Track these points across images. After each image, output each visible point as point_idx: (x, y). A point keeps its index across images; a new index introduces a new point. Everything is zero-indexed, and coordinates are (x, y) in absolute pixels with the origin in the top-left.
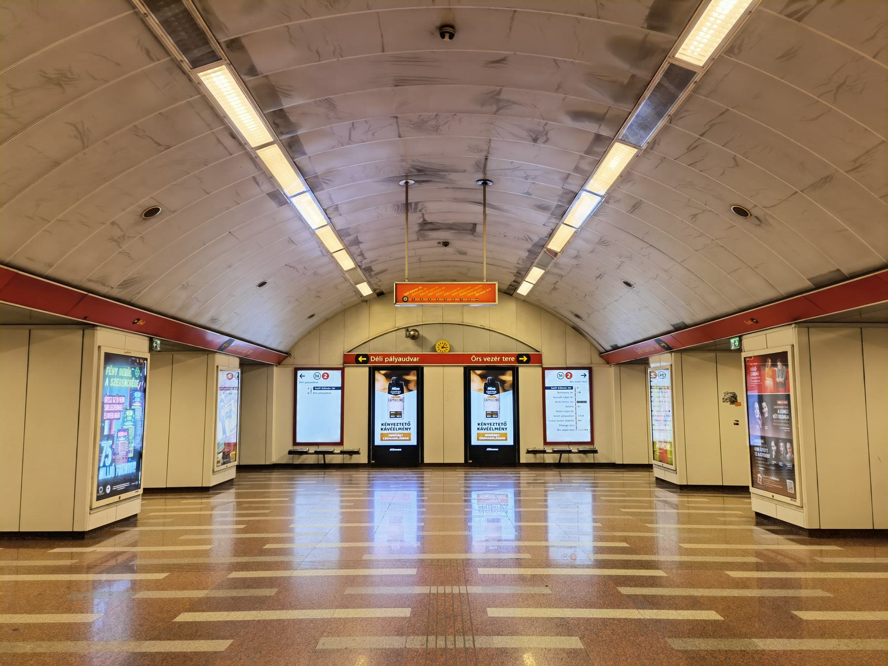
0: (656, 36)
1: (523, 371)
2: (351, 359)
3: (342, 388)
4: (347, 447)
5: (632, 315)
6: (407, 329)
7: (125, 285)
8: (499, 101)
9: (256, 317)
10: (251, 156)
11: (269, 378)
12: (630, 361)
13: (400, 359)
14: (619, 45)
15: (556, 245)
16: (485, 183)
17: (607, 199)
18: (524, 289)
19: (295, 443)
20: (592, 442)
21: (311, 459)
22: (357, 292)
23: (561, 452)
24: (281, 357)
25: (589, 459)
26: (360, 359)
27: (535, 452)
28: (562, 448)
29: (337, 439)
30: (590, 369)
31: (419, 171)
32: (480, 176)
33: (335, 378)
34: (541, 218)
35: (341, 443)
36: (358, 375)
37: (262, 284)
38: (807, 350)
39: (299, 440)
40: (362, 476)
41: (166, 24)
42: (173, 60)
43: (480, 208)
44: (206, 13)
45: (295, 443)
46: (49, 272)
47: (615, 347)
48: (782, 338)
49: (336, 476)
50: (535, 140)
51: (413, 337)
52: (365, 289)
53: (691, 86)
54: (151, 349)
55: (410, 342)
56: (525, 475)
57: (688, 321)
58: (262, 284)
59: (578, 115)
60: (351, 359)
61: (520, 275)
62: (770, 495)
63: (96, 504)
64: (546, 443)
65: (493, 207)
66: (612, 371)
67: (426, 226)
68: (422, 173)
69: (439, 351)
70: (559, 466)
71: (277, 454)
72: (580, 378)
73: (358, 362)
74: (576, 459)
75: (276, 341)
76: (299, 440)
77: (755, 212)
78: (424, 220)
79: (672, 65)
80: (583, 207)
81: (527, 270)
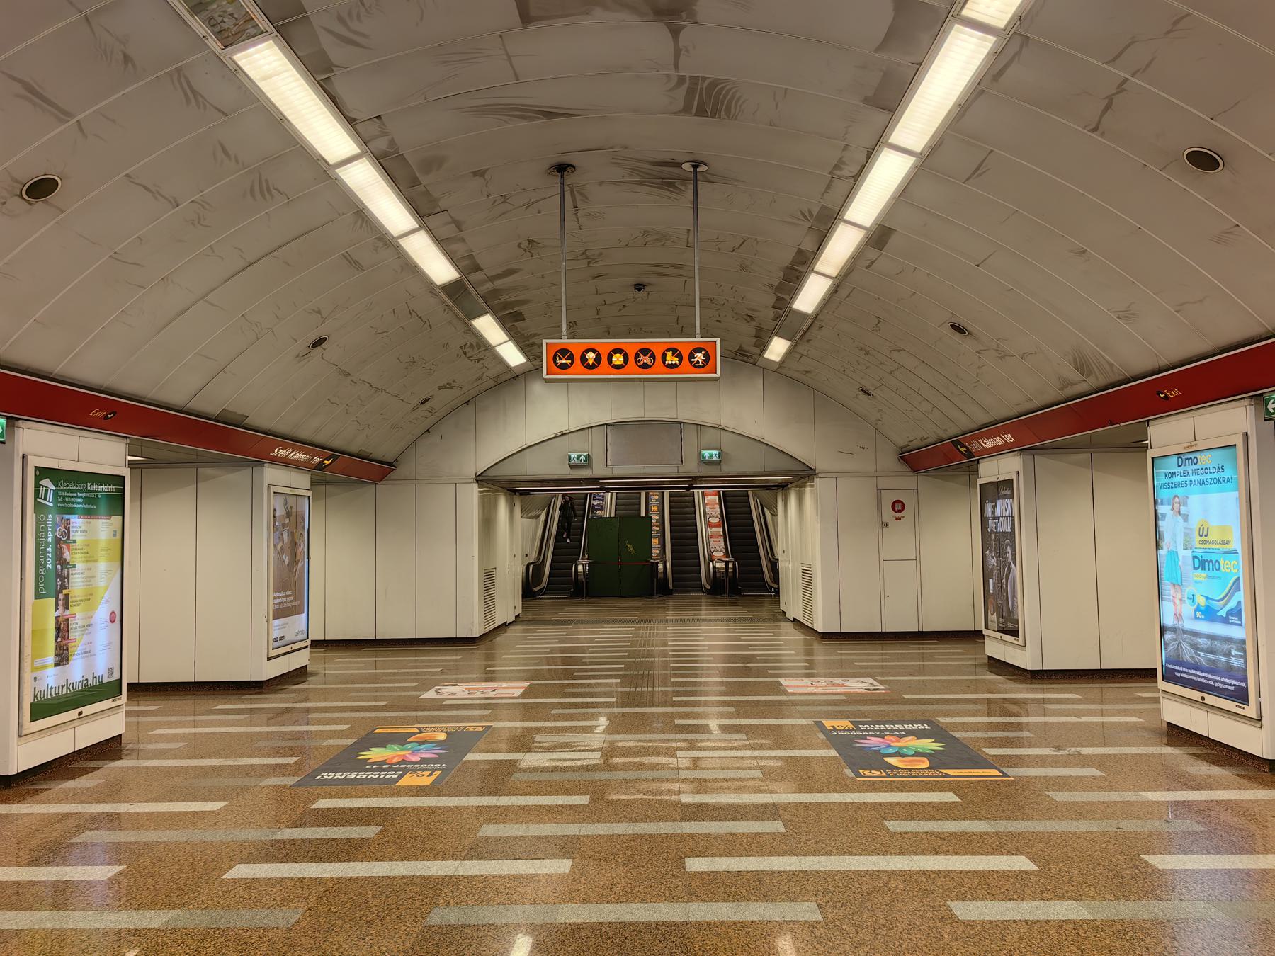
31: (672, 185)
32: (570, 179)
78: (675, 33)
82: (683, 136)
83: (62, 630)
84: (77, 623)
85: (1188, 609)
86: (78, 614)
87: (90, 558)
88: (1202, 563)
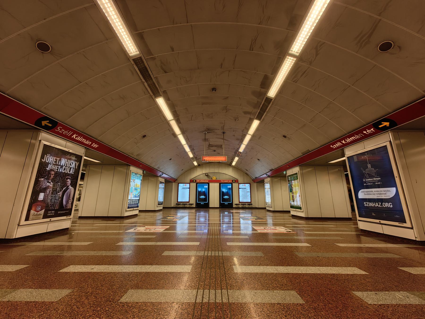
0: (263, 90)
1: (234, 184)
2: (192, 181)
3: (189, 188)
4: (190, 203)
5: (260, 170)
6: (205, 174)
7: (138, 155)
8: (227, 109)
9: (169, 171)
10: (167, 123)
11: (172, 186)
12: (260, 182)
14: (254, 93)
15: (241, 150)
16: (224, 133)
17: (253, 136)
18: (234, 164)
19: (178, 202)
20: (251, 202)
21: (181, 206)
22: (193, 164)
23: (243, 204)
24: (175, 180)
25: (250, 206)
27: (237, 204)
28: (243, 203)
29: (188, 201)
30: (250, 184)
33: (188, 186)
34: (237, 142)
35: (189, 202)
36: (194, 185)
37: (170, 159)
38: (302, 175)
39: (179, 201)
40: (194, 211)
41: (149, 85)
42: (150, 95)
43: (223, 140)
44: (158, 82)
45: (178, 202)
46: (119, 149)
47: (256, 178)
48: (296, 170)
49: (187, 211)
50: (235, 120)
51: (207, 176)
52: (195, 163)
53: (271, 103)
54: (143, 173)
55: (206, 177)
56: (234, 211)
57: (273, 168)
58: (170, 159)
59: (246, 113)
60: (192, 181)
61: (233, 160)
62: (295, 209)
63: (127, 210)
64: (240, 202)
65: (225, 140)
66: (255, 184)
67: (210, 146)
68: (209, 130)
69: (213, 179)
70: (243, 208)
71: (173, 205)
72: (248, 186)
74: (247, 206)
75: (173, 176)
76: (179, 201)
77: (288, 136)
79: (267, 98)
80: (248, 138)
81: (234, 158)
82: (208, 136)
83: (293, 197)
84: (295, 196)
85: (133, 196)
86: (295, 195)
87: (295, 187)
88: (136, 189)
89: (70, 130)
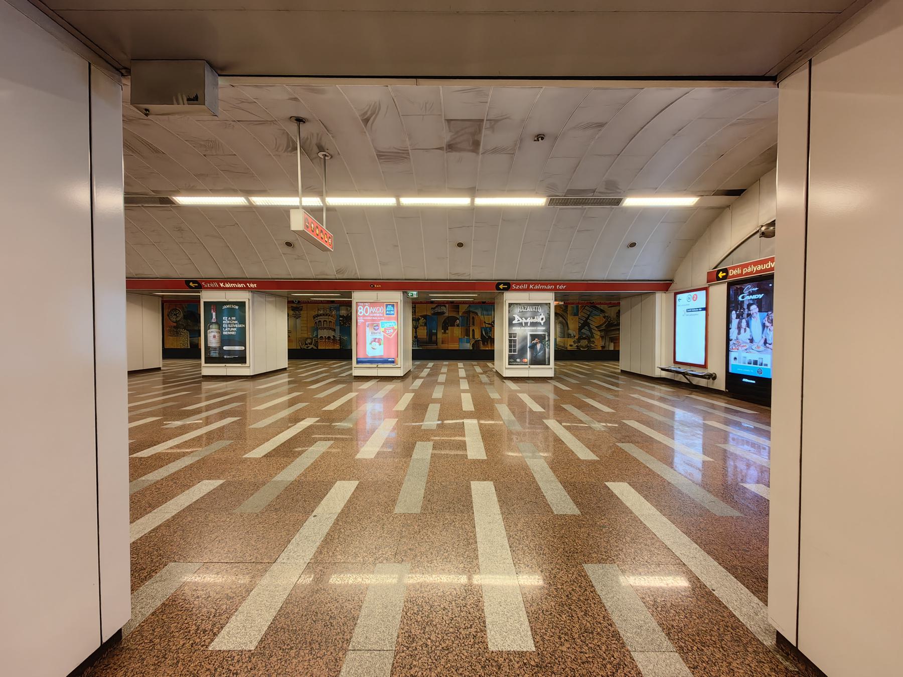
2: (713, 278)
4: (711, 370)
13: (760, 267)
26: (721, 275)
35: (705, 366)
45: (675, 362)
73: (718, 279)
89: (212, 282)
